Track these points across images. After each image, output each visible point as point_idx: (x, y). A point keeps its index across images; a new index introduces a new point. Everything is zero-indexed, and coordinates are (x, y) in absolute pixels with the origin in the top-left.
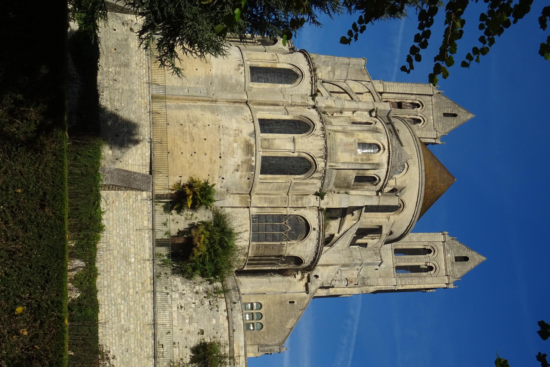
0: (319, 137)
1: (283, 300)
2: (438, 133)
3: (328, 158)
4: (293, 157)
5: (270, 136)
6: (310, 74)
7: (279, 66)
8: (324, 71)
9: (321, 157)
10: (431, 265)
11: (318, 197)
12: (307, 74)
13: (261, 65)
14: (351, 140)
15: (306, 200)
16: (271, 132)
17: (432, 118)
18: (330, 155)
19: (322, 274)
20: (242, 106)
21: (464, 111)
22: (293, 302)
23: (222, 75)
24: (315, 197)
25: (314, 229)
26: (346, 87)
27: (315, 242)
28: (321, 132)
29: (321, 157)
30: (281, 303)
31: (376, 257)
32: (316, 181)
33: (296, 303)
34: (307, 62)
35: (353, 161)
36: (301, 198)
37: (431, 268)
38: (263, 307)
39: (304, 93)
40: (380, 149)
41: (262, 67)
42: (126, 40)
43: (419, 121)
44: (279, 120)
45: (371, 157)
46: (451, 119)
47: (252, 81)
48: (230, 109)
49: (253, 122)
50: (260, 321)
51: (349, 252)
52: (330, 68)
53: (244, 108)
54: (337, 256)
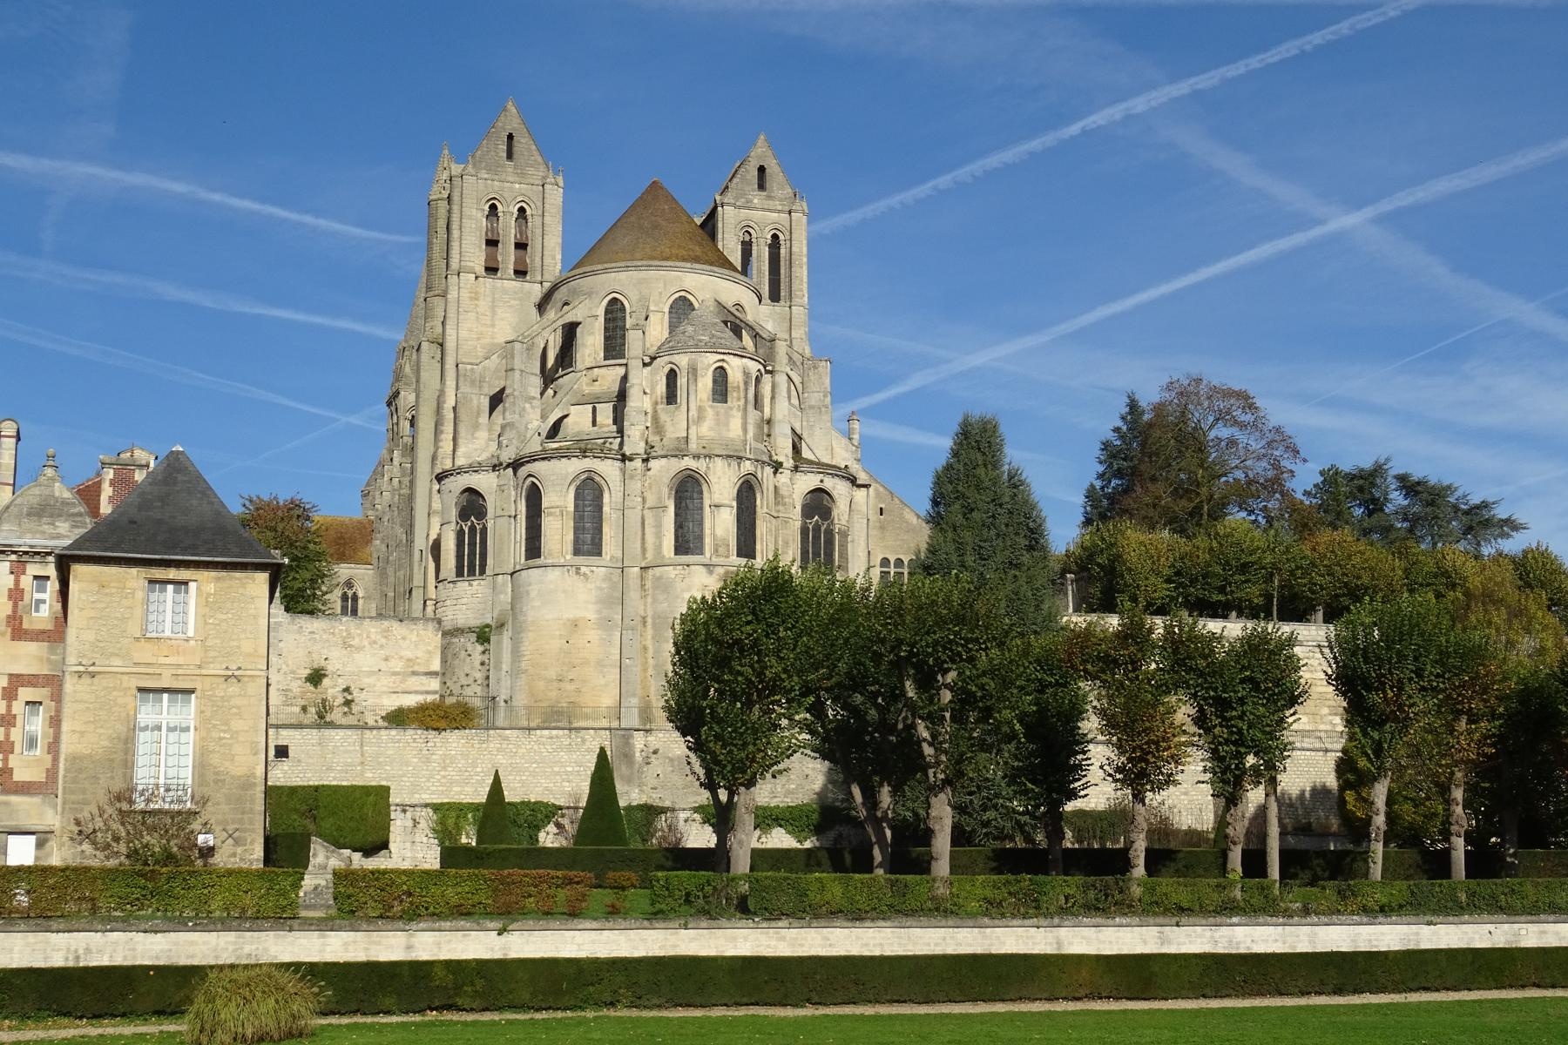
0: (710, 465)
1: (878, 524)
2: (548, 180)
3: (741, 454)
4: (738, 508)
5: (708, 540)
6: (587, 459)
7: (571, 508)
8: (531, 416)
9: (739, 464)
10: (769, 237)
11: (780, 470)
12: (588, 463)
13: (570, 536)
14: (710, 413)
15: (784, 491)
16: (701, 538)
17: (517, 186)
18: (736, 450)
19: (844, 459)
20: (650, 577)
21: (502, 118)
22: (881, 509)
23: (597, 603)
24: (778, 475)
25: (822, 481)
26: (498, 356)
27: (837, 480)
28: (702, 460)
29: (739, 464)
30: (882, 528)
31: (820, 369)
32: (765, 475)
33: (883, 506)
34: (563, 460)
35: (740, 414)
36: (783, 498)
37: (775, 237)
38: (887, 556)
39: (618, 472)
40: (721, 368)
41: (575, 533)
42: (671, 760)
43: (521, 210)
44: (675, 523)
45: (736, 385)
46: (517, 149)
47: (600, 554)
48: (661, 597)
49: (688, 566)
50: (906, 563)
51: (812, 411)
52: (527, 406)
53: (658, 575)
54: (818, 432)
